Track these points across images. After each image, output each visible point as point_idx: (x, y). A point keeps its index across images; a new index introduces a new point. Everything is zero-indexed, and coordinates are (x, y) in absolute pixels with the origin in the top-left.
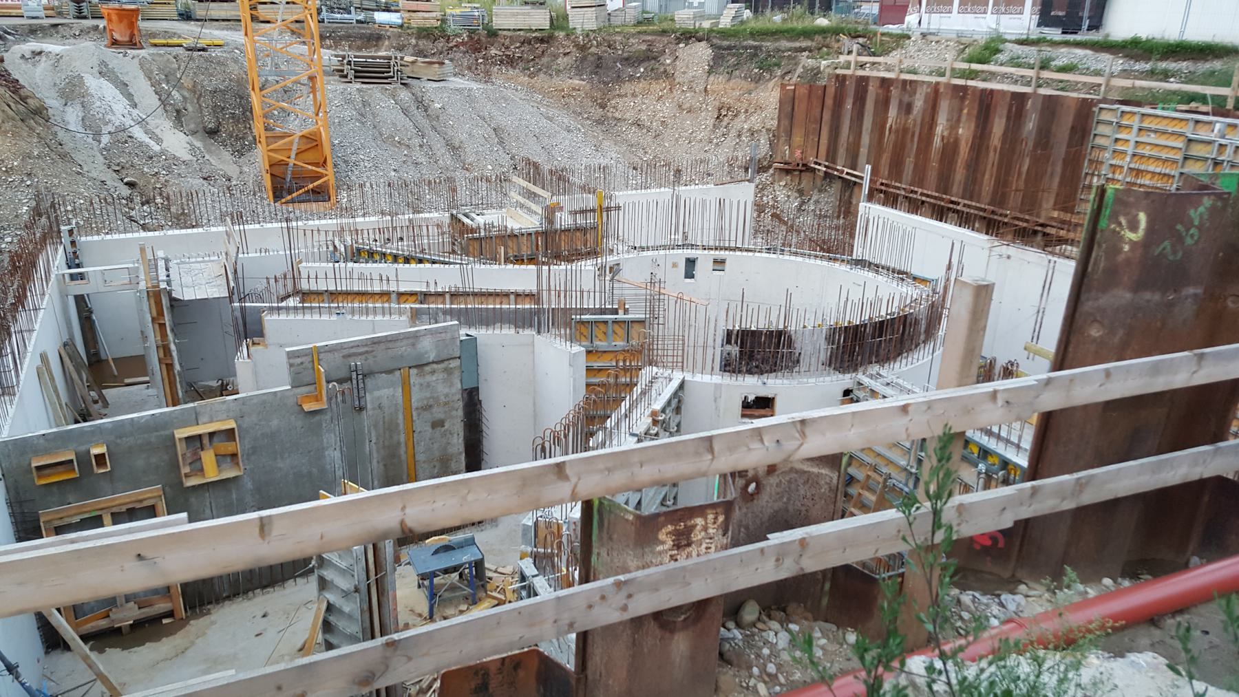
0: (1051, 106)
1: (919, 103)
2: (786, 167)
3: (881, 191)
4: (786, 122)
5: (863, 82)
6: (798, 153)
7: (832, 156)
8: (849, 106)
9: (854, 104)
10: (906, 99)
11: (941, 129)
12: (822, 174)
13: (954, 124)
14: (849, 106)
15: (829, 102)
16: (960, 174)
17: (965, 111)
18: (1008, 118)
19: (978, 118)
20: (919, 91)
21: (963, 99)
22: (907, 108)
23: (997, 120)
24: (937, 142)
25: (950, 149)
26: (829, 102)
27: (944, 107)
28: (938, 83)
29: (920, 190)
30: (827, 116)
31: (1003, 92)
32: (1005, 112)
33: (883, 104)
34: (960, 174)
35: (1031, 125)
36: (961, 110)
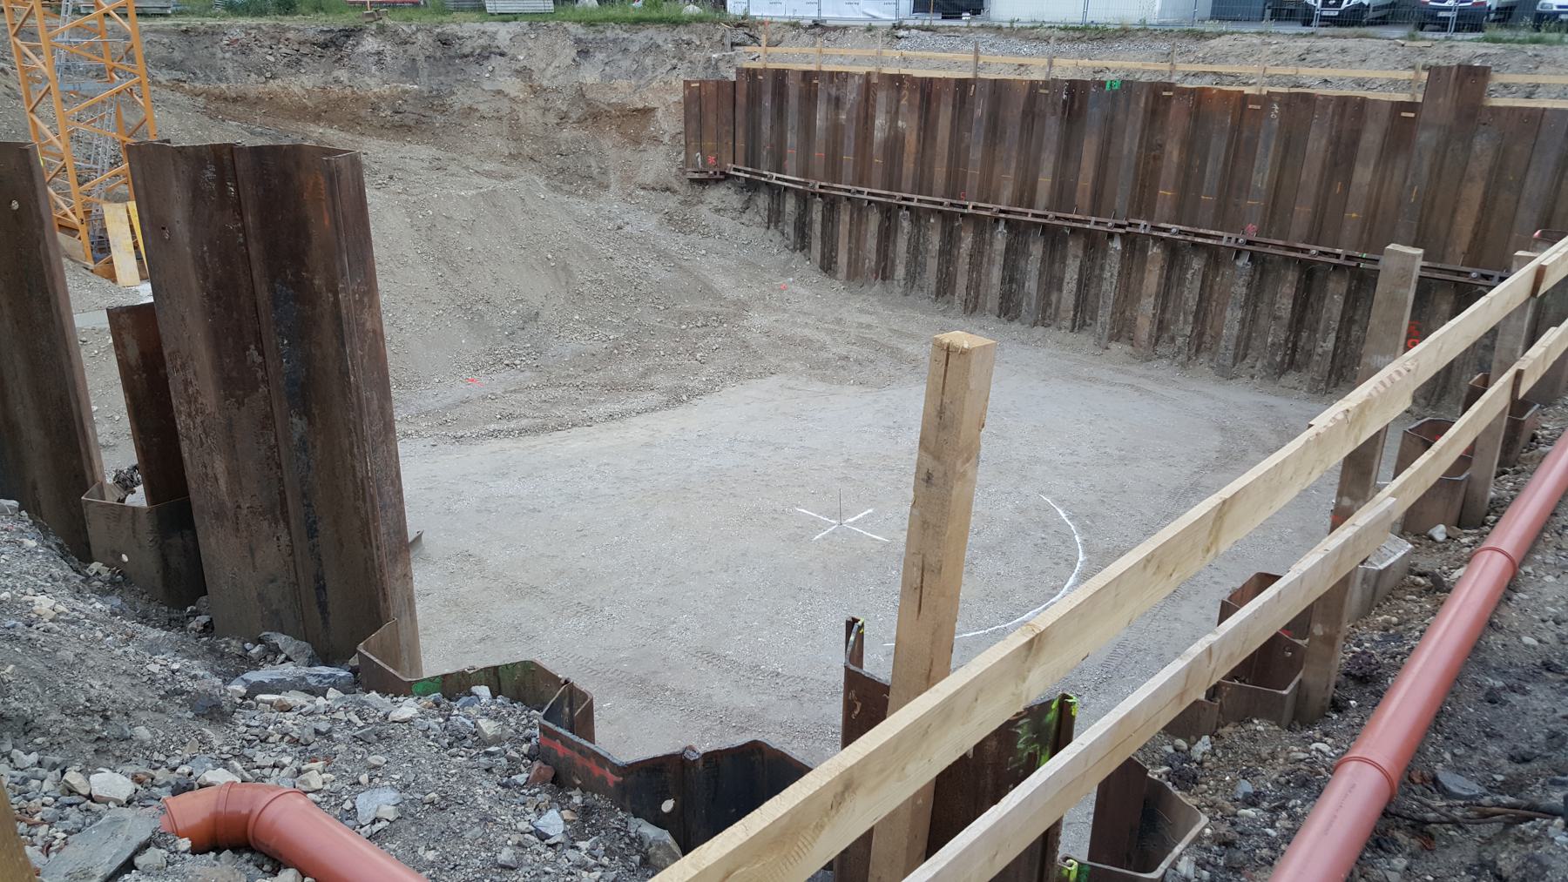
0: (998, 89)
1: (852, 95)
2: (704, 176)
3: (821, 195)
4: (694, 125)
5: (780, 76)
6: (711, 159)
7: (752, 160)
8: (767, 103)
9: (773, 100)
10: (834, 92)
11: (880, 121)
12: (742, 181)
13: (894, 115)
14: (767, 103)
15: (741, 99)
16: (909, 166)
17: (903, 102)
18: (954, 107)
19: (920, 108)
20: (850, 81)
21: (899, 89)
22: (837, 103)
23: (942, 108)
24: (878, 135)
25: (895, 144)
26: (741, 99)
27: (882, 98)
28: (868, 74)
29: (866, 190)
30: (740, 115)
31: (947, 80)
32: (950, 100)
33: (809, 97)
34: (909, 166)
35: (978, 112)
36: (898, 101)
